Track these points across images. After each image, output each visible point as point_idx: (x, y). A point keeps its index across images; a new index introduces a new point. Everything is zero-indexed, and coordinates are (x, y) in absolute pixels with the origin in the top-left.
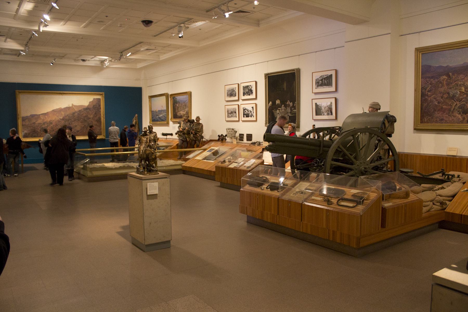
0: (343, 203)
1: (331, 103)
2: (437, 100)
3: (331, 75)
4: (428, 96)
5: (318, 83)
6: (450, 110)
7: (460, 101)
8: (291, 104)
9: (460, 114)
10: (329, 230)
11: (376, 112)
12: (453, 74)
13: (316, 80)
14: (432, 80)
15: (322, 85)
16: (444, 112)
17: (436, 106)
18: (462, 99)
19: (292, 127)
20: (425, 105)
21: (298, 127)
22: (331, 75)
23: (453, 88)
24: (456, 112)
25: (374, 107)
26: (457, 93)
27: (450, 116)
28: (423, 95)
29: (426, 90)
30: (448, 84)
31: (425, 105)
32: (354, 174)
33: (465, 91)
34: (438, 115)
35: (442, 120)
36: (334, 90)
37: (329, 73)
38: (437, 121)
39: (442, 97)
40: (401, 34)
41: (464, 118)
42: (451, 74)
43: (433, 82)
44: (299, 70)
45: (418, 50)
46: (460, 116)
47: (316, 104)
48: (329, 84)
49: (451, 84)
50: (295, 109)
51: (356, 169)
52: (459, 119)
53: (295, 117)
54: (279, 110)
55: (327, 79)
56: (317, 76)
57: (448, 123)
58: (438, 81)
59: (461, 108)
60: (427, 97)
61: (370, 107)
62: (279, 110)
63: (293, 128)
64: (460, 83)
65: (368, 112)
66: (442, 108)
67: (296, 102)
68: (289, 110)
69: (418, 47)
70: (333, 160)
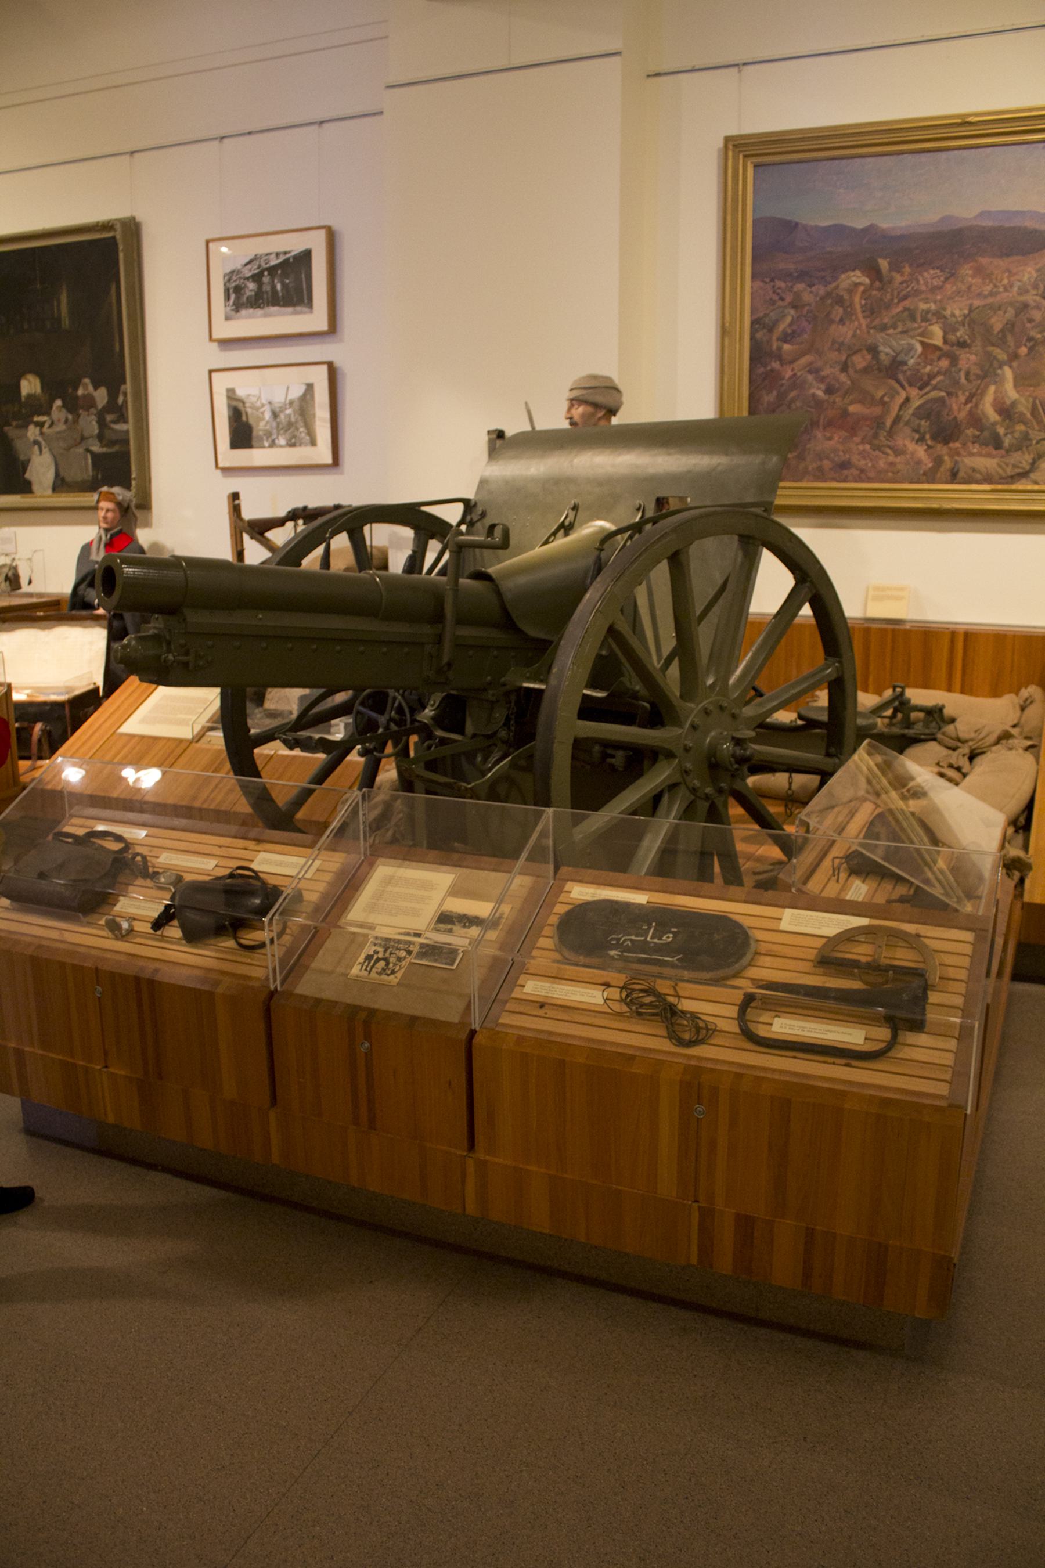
0: (784, 1026)
1: (310, 387)
2: (822, 380)
3: (306, 256)
4: (779, 357)
5: (238, 290)
6: (878, 423)
7: (923, 383)
8: (101, 396)
9: (921, 440)
10: (707, 1214)
11: (603, 423)
12: (895, 267)
13: (229, 276)
14: (800, 286)
15: (260, 300)
16: (853, 431)
17: (818, 404)
18: (931, 376)
19: (119, 504)
20: (768, 398)
21: (145, 504)
22: (306, 256)
23: (895, 327)
24: (907, 430)
25: (599, 399)
26: (911, 348)
27: (878, 448)
28: (759, 354)
29: (771, 330)
30: (871, 311)
31: (768, 398)
32: (677, 778)
33: (945, 341)
34: (826, 442)
35: (845, 465)
36: (324, 326)
37: (295, 245)
38: (820, 469)
39: (845, 368)
40: (654, 68)
41: (938, 461)
42: (884, 264)
43: (807, 297)
44: (132, 229)
45: (741, 149)
46: (921, 452)
47: (231, 394)
48: (297, 296)
49: (888, 307)
50: (122, 418)
51: (687, 750)
52: (919, 462)
53: (125, 456)
54: (41, 425)
55: (285, 275)
56: (230, 256)
57: (870, 480)
58: (828, 294)
59: (928, 417)
60: (776, 365)
61: (573, 402)
62: (41, 425)
63: (124, 510)
64: (923, 306)
65: (569, 427)
66: (845, 413)
67: (128, 387)
68: (89, 424)
69: (733, 131)
70: (589, 710)
